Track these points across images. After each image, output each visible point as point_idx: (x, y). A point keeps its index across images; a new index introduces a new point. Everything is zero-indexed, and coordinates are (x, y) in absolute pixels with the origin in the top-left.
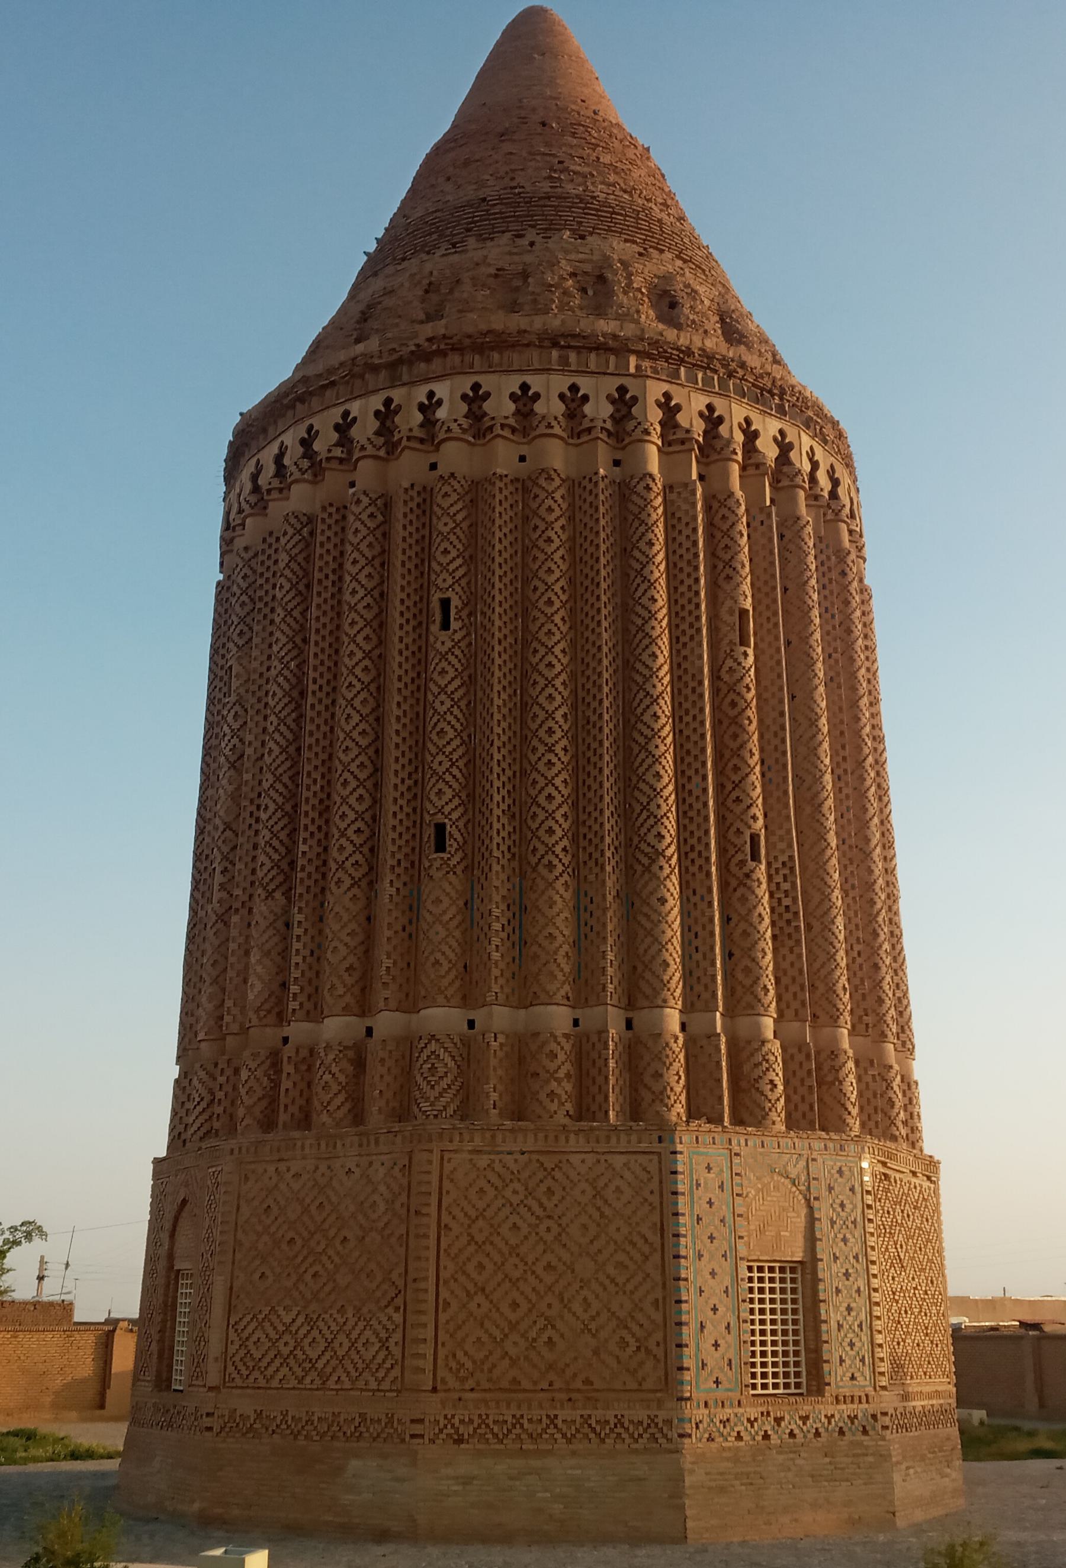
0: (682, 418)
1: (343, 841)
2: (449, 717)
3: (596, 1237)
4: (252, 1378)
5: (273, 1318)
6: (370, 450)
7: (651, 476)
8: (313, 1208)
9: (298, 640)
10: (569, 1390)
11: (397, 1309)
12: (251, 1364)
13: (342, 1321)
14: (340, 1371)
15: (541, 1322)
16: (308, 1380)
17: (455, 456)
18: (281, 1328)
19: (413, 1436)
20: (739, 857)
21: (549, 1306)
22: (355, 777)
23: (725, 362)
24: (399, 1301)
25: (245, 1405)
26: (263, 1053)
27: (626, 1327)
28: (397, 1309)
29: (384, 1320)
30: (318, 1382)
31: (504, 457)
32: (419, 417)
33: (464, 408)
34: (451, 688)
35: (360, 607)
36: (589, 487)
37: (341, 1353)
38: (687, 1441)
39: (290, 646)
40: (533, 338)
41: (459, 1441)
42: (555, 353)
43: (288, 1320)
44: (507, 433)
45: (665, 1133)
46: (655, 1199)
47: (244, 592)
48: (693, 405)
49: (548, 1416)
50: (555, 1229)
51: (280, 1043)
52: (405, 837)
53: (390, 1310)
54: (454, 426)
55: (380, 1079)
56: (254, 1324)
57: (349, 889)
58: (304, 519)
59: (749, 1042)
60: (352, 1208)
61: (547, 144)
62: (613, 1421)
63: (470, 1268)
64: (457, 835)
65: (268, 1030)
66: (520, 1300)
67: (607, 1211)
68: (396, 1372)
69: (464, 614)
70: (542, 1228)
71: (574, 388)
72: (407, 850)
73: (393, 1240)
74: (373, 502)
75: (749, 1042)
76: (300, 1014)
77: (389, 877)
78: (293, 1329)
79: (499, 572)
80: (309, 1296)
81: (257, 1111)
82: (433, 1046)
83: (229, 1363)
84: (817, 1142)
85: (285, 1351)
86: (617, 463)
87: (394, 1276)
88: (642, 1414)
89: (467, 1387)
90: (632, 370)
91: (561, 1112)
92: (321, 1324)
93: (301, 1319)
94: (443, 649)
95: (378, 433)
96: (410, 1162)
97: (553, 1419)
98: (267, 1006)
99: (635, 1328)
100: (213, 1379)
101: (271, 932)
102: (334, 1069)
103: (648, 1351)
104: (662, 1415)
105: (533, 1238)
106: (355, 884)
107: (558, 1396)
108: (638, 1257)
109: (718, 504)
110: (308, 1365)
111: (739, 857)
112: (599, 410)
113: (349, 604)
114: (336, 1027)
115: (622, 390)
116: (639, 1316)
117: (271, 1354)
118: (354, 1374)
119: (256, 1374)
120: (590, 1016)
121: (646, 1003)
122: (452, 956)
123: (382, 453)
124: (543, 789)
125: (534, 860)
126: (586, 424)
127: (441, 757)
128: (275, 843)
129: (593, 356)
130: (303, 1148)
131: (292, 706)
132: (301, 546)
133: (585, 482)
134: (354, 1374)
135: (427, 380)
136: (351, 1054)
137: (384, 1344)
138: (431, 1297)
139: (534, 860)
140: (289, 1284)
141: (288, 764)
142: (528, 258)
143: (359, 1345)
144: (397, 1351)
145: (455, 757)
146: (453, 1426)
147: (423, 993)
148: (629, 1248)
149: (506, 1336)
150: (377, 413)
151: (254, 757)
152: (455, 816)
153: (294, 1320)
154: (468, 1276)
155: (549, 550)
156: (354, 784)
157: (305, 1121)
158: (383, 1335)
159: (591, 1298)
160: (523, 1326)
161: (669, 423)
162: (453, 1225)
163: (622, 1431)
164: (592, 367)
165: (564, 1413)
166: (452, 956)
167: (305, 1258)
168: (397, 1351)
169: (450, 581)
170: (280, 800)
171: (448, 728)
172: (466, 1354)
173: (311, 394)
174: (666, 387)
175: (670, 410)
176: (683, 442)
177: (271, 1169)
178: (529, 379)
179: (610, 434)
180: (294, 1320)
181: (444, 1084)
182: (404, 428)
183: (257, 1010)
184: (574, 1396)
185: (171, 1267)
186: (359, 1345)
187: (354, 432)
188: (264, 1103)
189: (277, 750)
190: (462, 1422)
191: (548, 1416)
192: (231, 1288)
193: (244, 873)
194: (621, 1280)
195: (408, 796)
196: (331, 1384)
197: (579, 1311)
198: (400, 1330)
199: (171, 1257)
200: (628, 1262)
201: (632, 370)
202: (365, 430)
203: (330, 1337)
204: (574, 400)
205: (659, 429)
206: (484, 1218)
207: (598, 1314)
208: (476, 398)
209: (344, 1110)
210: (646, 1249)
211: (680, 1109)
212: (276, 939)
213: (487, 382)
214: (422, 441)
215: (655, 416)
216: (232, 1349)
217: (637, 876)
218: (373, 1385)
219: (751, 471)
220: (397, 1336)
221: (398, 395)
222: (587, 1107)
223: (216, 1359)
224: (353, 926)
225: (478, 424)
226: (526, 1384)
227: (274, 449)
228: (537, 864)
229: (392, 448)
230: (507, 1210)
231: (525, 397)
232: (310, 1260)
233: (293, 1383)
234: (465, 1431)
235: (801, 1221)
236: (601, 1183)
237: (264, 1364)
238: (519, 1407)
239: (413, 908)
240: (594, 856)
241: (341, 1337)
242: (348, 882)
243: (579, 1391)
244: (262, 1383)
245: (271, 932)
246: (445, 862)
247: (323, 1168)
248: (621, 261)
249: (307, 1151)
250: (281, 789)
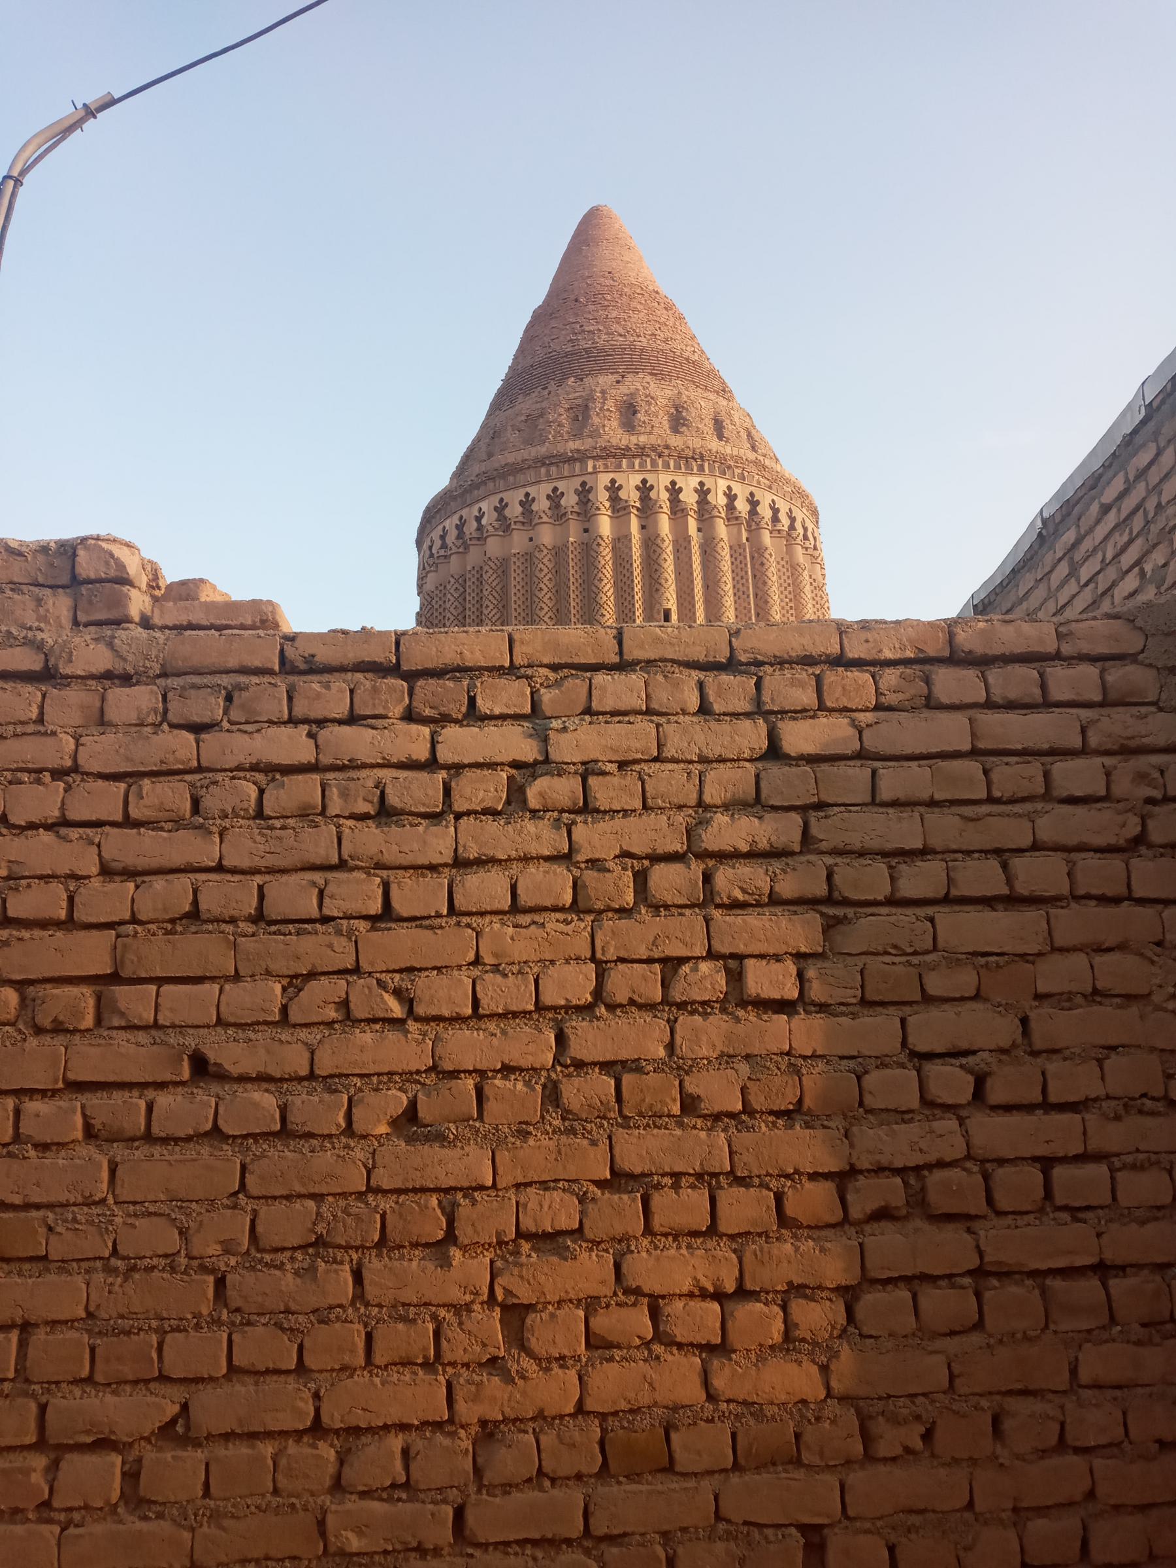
0: (622, 494)
6: (454, 550)
7: (601, 537)
23: (654, 449)
31: (518, 542)
32: (475, 524)
33: (496, 515)
40: (530, 463)
42: (543, 470)
44: (519, 526)
48: (630, 482)
54: (490, 528)
61: (576, 315)
71: (555, 489)
74: (457, 581)
79: (515, 614)
86: (586, 531)
90: (590, 469)
95: (458, 538)
109: (651, 544)
112: (570, 501)
115: (584, 484)
123: (461, 550)
126: (563, 511)
129: (566, 466)
135: (478, 501)
142: (545, 404)
155: (540, 596)
161: (615, 499)
164: (566, 474)
174: (612, 475)
175: (614, 489)
178: (529, 490)
179: (578, 514)
182: (467, 533)
201: (590, 469)
204: (555, 497)
205: (607, 504)
208: (501, 509)
213: (507, 496)
215: (603, 496)
219: (679, 515)
229: (467, 548)
231: (527, 502)
248: (603, 392)
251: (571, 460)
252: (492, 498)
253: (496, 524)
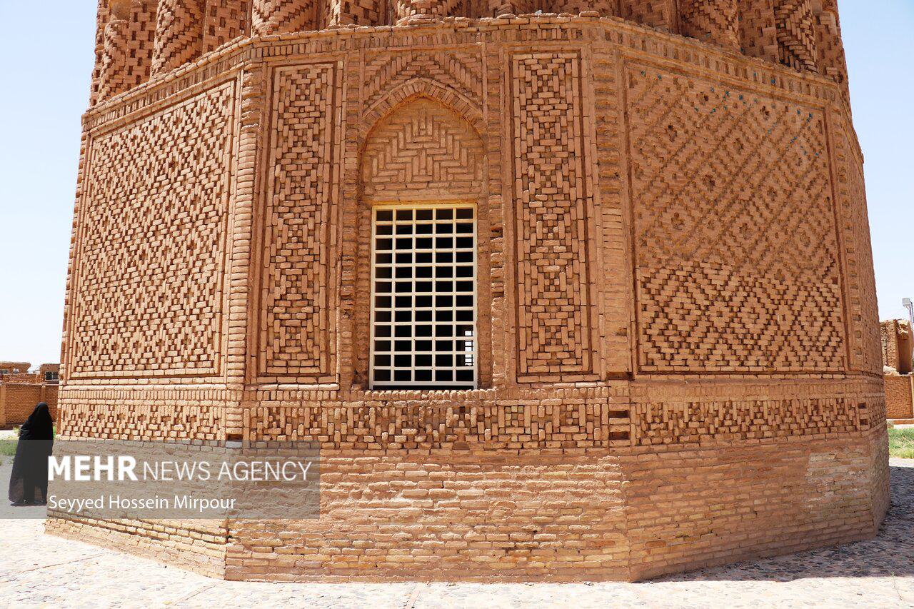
11: (835, 282)
14: (786, 349)
16: (751, 362)
18: (710, 292)
24: (835, 270)
25: (676, 399)
28: (835, 282)
56: (673, 284)
73: (821, 201)
78: (726, 294)
83: (643, 338)
85: (720, 323)
92: (758, 290)
93: (734, 283)
100: (617, 355)
110: (749, 342)
119: (684, 352)
140: (713, 235)
190: (480, 418)
192: (633, 231)
196: (779, 366)
203: (771, 307)
220: (838, 311)
233: (734, 365)
244: (694, 366)
247: (734, 95)
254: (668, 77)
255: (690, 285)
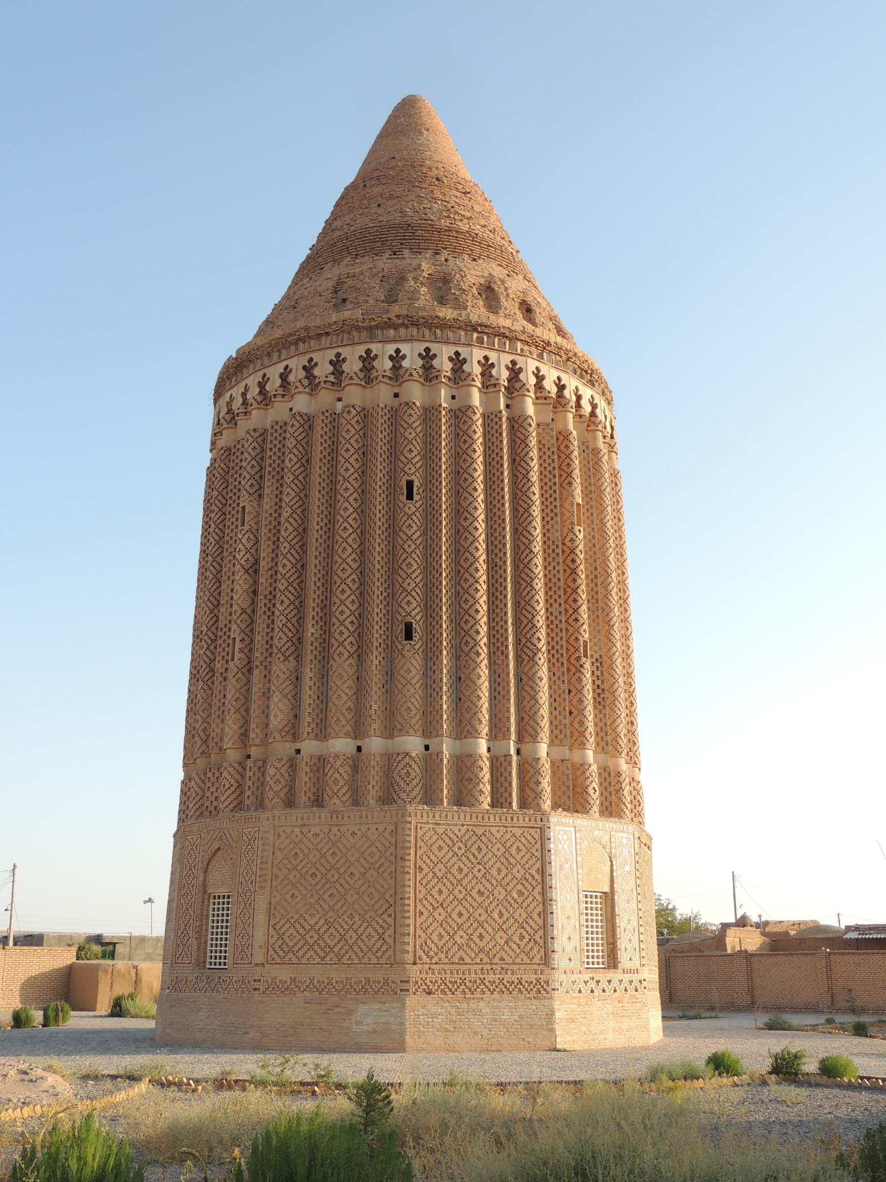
1: (342, 628)
2: (414, 555)
3: (507, 875)
4: (287, 958)
5: (302, 921)
8: (328, 855)
9: (302, 495)
10: (492, 964)
12: (286, 949)
13: (351, 923)
14: (351, 953)
15: (475, 925)
16: (328, 959)
17: (416, 393)
18: (308, 927)
19: (401, 990)
20: (577, 655)
21: (480, 915)
22: (350, 588)
24: (391, 911)
25: (283, 974)
26: (285, 759)
27: (523, 928)
28: (390, 916)
29: (381, 922)
30: (335, 959)
32: (389, 364)
33: (420, 362)
34: (415, 537)
35: (351, 479)
36: (495, 420)
37: (351, 942)
38: (556, 992)
39: (297, 499)
41: (429, 993)
42: (475, 335)
43: (312, 922)
45: (543, 817)
46: (538, 854)
47: (254, 458)
49: (480, 979)
50: (483, 871)
51: (294, 753)
52: (383, 629)
53: (385, 916)
54: (414, 373)
55: (304, 778)
56: (288, 925)
57: (347, 659)
58: (306, 418)
59: (582, 765)
60: (357, 855)
62: (516, 981)
63: (435, 892)
64: (419, 631)
65: (287, 744)
66: (464, 911)
67: (512, 861)
68: (389, 953)
69: (421, 491)
70: (476, 870)
72: (384, 637)
73: (386, 875)
74: (358, 413)
75: (582, 765)
76: (312, 735)
77: (375, 653)
78: (317, 928)
80: (327, 908)
81: (282, 795)
82: (407, 759)
83: (270, 949)
84: (611, 824)
85: (311, 941)
87: (387, 896)
88: (533, 978)
89: (434, 961)
91: (486, 801)
92: (336, 925)
94: (410, 512)
96: (396, 828)
97: (482, 981)
98: (286, 729)
99: (528, 928)
101: (288, 682)
102: (341, 770)
103: (536, 942)
104: (543, 978)
105: (471, 875)
106: (351, 656)
107: (485, 967)
108: (529, 888)
110: (328, 950)
111: (577, 655)
113: (343, 477)
114: (342, 745)
116: (530, 921)
117: (302, 943)
118: (361, 954)
119: (291, 955)
120: (498, 746)
121: (531, 740)
122: (417, 706)
123: (363, 383)
124: (472, 605)
125: (466, 650)
127: (408, 580)
128: (289, 625)
130: (320, 818)
131: (299, 538)
132: (304, 434)
133: (493, 417)
134: (361, 954)
135: (395, 341)
136: (350, 762)
137: (381, 937)
138: (412, 908)
139: (466, 650)
140: (313, 901)
141: (296, 575)
143: (364, 937)
144: (390, 941)
145: (417, 580)
146: (426, 984)
147: (399, 727)
148: (524, 882)
149: (456, 932)
150: (361, 356)
151: (266, 568)
152: (418, 618)
153: (317, 923)
154: (433, 897)
156: (349, 592)
157: (318, 801)
158: (381, 931)
159: (504, 911)
160: (465, 927)
161: (539, 386)
162: (424, 866)
163: (521, 987)
165: (491, 977)
166: (417, 706)
167: (324, 885)
168: (390, 941)
169: (413, 470)
170: (292, 598)
171: (413, 562)
172: (433, 942)
173: (310, 337)
174: (537, 364)
176: (495, 385)
177: (297, 830)
178: (460, 349)
180: (317, 923)
181: (414, 783)
183: (280, 732)
184: (494, 967)
185: (205, 892)
186: (364, 937)
187: (345, 367)
188: (285, 790)
189: (289, 566)
191: (480, 979)
192: (270, 904)
193: (261, 643)
194: (520, 900)
195: (385, 603)
196: (345, 960)
197: (496, 917)
198: (392, 929)
199: (205, 885)
200: (523, 890)
202: (352, 366)
203: (343, 932)
206: (442, 863)
207: (507, 920)
209: (347, 796)
210: (534, 883)
211: (549, 802)
212: (291, 687)
214: (390, 378)
216: (272, 941)
217: (525, 663)
218: (374, 961)
220: (390, 932)
221: (375, 348)
222: (499, 800)
223: (261, 947)
224: (350, 682)
225: (429, 373)
226: (467, 960)
227: (280, 368)
228: (469, 652)
230: (455, 859)
232: (328, 885)
233: (318, 960)
234: (433, 988)
235: (607, 869)
236: (508, 844)
237: (296, 949)
238: (464, 974)
239: (390, 674)
240: (501, 649)
241: (351, 933)
242: (346, 655)
243: (497, 964)
244: (295, 960)
245: (288, 682)
246: (413, 647)
247: (334, 830)
249: (323, 820)
250: (293, 591)
251: (504, 336)
252: (416, 344)
253: (421, 371)
254: (297, 830)
255: (297, 925)
